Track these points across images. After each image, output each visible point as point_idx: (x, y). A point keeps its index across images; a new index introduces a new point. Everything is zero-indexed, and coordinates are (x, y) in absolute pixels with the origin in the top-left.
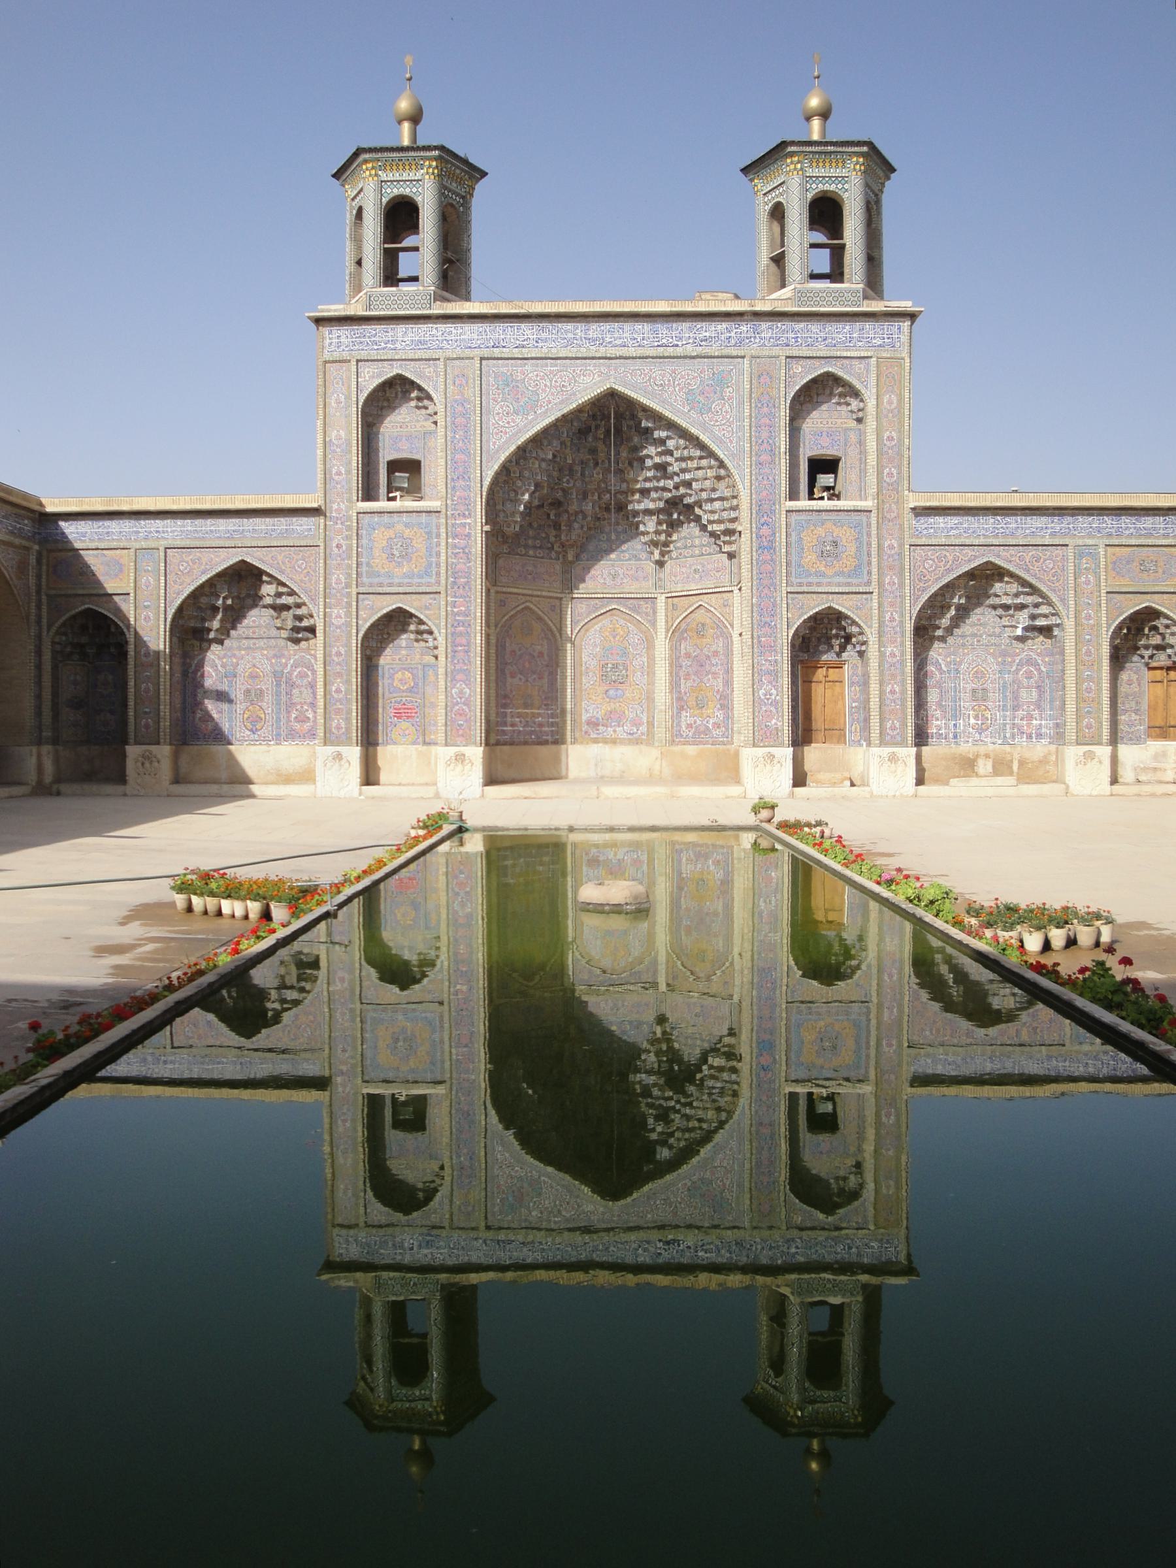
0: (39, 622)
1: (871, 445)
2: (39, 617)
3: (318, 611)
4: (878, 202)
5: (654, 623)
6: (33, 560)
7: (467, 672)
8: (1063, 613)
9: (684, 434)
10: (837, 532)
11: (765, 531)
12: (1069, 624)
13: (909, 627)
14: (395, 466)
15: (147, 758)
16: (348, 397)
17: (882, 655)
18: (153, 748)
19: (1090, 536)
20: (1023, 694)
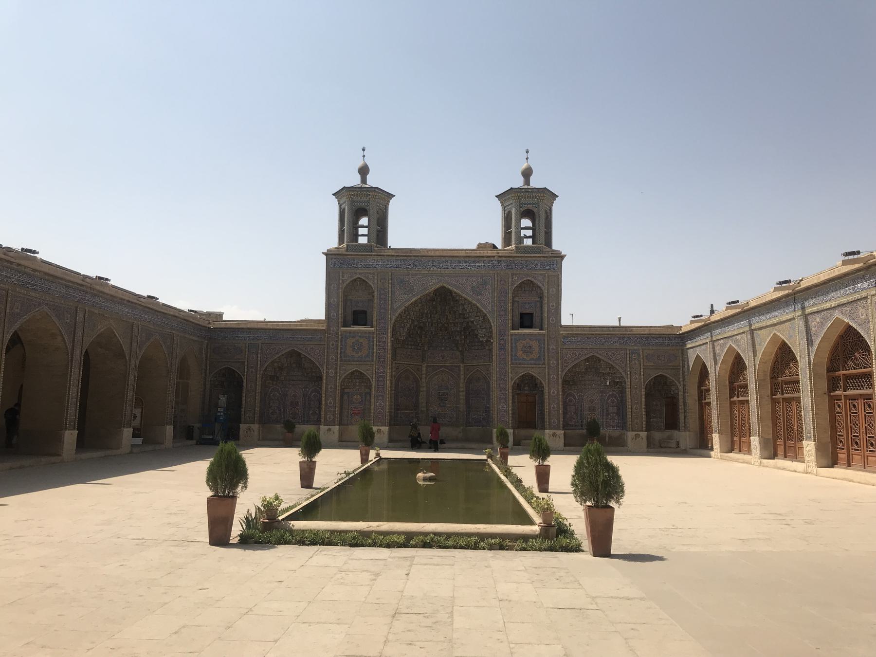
0: (205, 372)
1: (545, 309)
2: (206, 370)
3: (324, 371)
4: (551, 210)
5: (459, 377)
6: (205, 346)
7: (383, 396)
8: (625, 376)
9: (470, 303)
10: (531, 343)
11: (502, 342)
12: (628, 381)
13: (560, 381)
14: (355, 313)
15: (249, 429)
16: (338, 286)
17: (549, 392)
18: (252, 426)
19: (635, 345)
20: (611, 409)
